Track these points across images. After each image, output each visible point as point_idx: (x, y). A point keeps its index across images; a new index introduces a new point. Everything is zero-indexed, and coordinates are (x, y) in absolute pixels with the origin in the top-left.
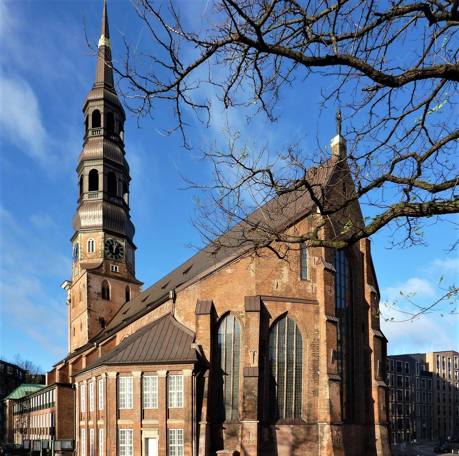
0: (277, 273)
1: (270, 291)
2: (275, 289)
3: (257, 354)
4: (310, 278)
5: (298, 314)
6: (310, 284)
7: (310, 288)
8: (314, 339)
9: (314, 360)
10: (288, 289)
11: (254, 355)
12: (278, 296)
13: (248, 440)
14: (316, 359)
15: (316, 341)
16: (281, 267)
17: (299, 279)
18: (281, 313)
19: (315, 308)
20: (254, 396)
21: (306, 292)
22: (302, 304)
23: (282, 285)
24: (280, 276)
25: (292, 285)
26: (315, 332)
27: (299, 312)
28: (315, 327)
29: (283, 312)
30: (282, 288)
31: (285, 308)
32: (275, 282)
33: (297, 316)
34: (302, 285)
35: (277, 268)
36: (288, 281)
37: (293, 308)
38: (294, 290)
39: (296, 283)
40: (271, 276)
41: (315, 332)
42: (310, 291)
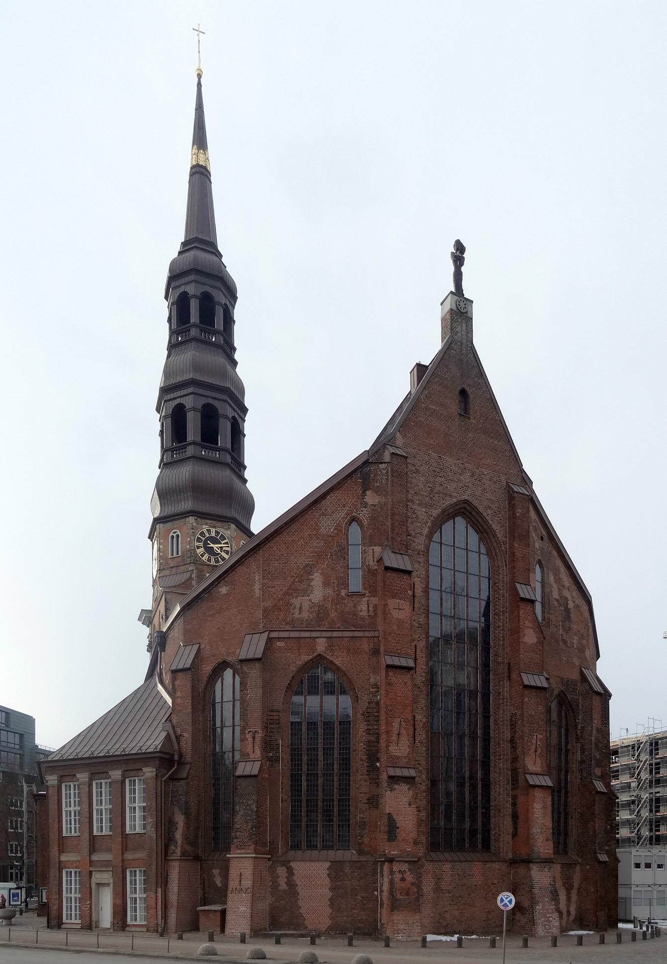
1: (288, 620)
2: (297, 616)
3: (259, 737)
4: (365, 589)
5: (340, 659)
7: (365, 608)
8: (369, 703)
9: (369, 742)
11: (254, 738)
13: (238, 887)
14: (373, 738)
16: (310, 574)
18: (306, 658)
20: (252, 811)
21: (356, 615)
24: (306, 592)
26: (372, 690)
28: (372, 680)
29: (310, 657)
31: (313, 649)
32: (296, 602)
35: (302, 575)
36: (322, 599)
37: (330, 647)
38: (333, 614)
40: (291, 592)
41: (372, 690)
42: (364, 614)
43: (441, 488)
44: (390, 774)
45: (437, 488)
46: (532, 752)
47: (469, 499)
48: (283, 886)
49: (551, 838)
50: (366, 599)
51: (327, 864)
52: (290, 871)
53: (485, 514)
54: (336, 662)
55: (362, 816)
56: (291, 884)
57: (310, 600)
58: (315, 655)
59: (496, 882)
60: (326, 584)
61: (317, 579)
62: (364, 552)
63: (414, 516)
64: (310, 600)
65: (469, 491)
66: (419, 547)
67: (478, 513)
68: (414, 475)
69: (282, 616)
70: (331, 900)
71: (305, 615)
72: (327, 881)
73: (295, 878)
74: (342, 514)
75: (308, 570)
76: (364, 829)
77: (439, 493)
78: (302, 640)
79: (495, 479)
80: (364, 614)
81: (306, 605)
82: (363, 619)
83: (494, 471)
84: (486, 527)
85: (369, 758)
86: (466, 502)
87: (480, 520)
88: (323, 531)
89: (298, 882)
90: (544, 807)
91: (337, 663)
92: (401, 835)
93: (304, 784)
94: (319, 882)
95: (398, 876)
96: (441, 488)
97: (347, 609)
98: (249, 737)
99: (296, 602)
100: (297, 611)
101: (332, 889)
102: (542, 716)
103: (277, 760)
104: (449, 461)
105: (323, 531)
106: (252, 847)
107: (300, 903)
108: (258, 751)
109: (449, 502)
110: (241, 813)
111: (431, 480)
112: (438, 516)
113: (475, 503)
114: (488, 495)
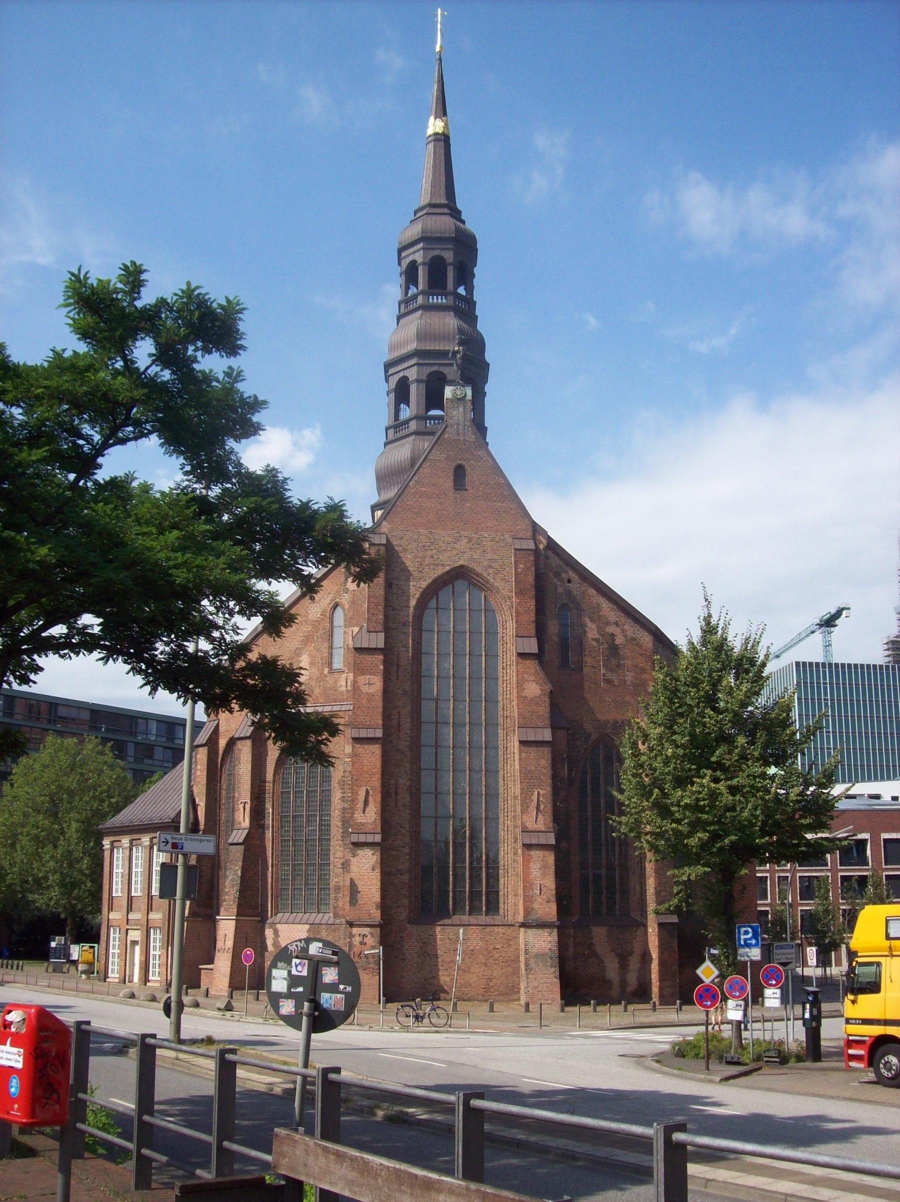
3: (248, 806)
4: (344, 666)
6: (344, 675)
7: (344, 683)
16: (299, 655)
17: (326, 671)
21: (336, 691)
34: (330, 680)
42: (343, 689)
43: (431, 561)
44: (353, 840)
45: (427, 561)
47: (466, 563)
49: (553, 899)
50: (345, 675)
51: (307, 927)
52: (276, 932)
53: (485, 574)
62: (345, 632)
67: (478, 575)
73: (279, 939)
76: (338, 893)
77: (429, 565)
79: (497, 539)
80: (343, 689)
82: (342, 693)
83: (497, 531)
85: (343, 825)
86: (462, 566)
87: (481, 580)
92: (362, 899)
95: (357, 940)
96: (431, 561)
98: (241, 806)
106: (235, 910)
109: (440, 571)
110: (230, 878)
114: (489, 556)
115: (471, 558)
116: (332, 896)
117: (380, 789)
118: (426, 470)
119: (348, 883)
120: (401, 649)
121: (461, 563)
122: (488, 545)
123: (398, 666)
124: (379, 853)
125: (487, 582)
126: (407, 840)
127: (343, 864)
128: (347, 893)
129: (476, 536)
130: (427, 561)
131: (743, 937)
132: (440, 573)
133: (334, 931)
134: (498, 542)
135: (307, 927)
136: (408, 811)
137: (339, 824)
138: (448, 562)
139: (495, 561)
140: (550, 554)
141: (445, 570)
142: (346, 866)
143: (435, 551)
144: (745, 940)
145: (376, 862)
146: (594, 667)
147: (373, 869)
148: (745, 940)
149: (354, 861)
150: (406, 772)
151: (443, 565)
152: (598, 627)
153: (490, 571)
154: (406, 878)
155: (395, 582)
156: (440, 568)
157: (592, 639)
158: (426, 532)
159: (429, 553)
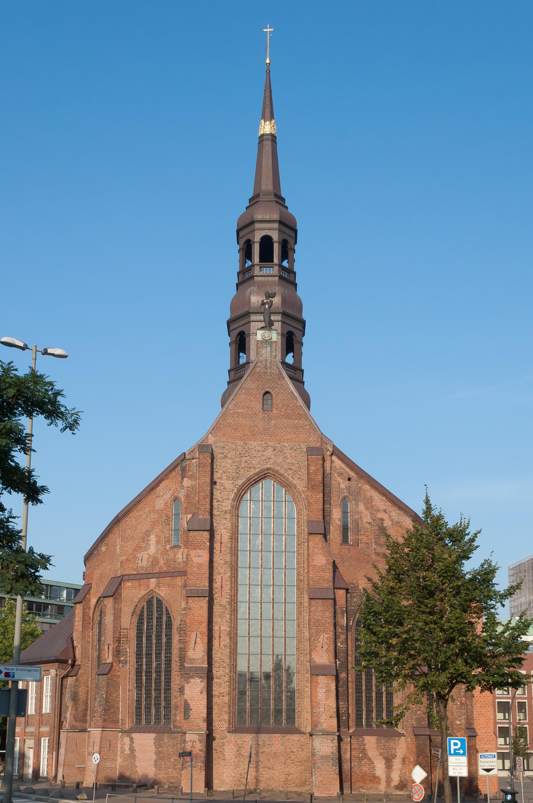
0: (144, 545)
2: (140, 565)
3: (111, 647)
5: (164, 592)
6: (181, 550)
10: (155, 561)
12: (143, 572)
13: (92, 752)
15: (183, 623)
16: (148, 536)
18: (143, 593)
19: (183, 581)
21: (175, 562)
22: (168, 578)
23: (148, 559)
24: (146, 549)
25: (159, 556)
27: (164, 588)
30: (148, 562)
31: (148, 586)
32: (139, 555)
33: (162, 594)
36: (155, 552)
37: (158, 585)
38: (161, 562)
39: (165, 552)
40: (138, 549)
42: (180, 560)
45: (243, 465)
46: (319, 647)
47: (272, 466)
48: (127, 752)
50: (182, 550)
52: (132, 740)
53: (286, 474)
54: (161, 594)
55: (175, 700)
56: (132, 750)
57: (148, 554)
58: (149, 590)
59: (295, 750)
60: (158, 542)
61: (153, 538)
63: (222, 487)
64: (148, 554)
65: (272, 461)
66: (226, 508)
67: (280, 474)
68: (223, 460)
69: (131, 566)
70: (156, 761)
71: (145, 564)
72: (153, 748)
73: (134, 745)
74: (169, 494)
75: (147, 534)
78: (142, 581)
79: (295, 448)
80: (180, 560)
81: (145, 557)
84: (288, 483)
87: (282, 479)
88: (157, 507)
89: (136, 749)
90: (328, 691)
91: (162, 595)
93: (144, 678)
94: (148, 748)
96: (246, 464)
97: (170, 558)
99: (139, 555)
100: (140, 561)
101: (157, 753)
102: (329, 620)
103: (126, 663)
104: (254, 444)
105: (157, 507)
107: (137, 763)
108: (110, 657)
109: (252, 472)
111: (238, 460)
112: (243, 484)
113: (277, 468)
114: (289, 461)
115: (275, 463)
116: (173, 712)
117: (207, 634)
118: (242, 397)
119: (183, 703)
120: (223, 531)
121: (268, 466)
122: (288, 452)
123: (221, 543)
124: (206, 680)
125: (288, 480)
126: (227, 671)
127: (180, 689)
128: (182, 710)
129: (279, 445)
130: (243, 465)
131: (453, 747)
132: (252, 473)
133: (173, 738)
134: (295, 450)
135: (154, 735)
136: (228, 650)
137: (177, 659)
138: (258, 466)
139: (293, 464)
140: (334, 458)
141: (256, 472)
142: (182, 690)
143: (248, 458)
144: (455, 750)
145: (203, 687)
146: (368, 544)
147: (201, 693)
148: (455, 750)
149: (187, 686)
150: (227, 621)
151: (254, 468)
152: (370, 513)
153: (290, 472)
154: (226, 699)
155: (218, 481)
156: (252, 470)
157: (366, 522)
158: (242, 443)
159: (244, 459)
